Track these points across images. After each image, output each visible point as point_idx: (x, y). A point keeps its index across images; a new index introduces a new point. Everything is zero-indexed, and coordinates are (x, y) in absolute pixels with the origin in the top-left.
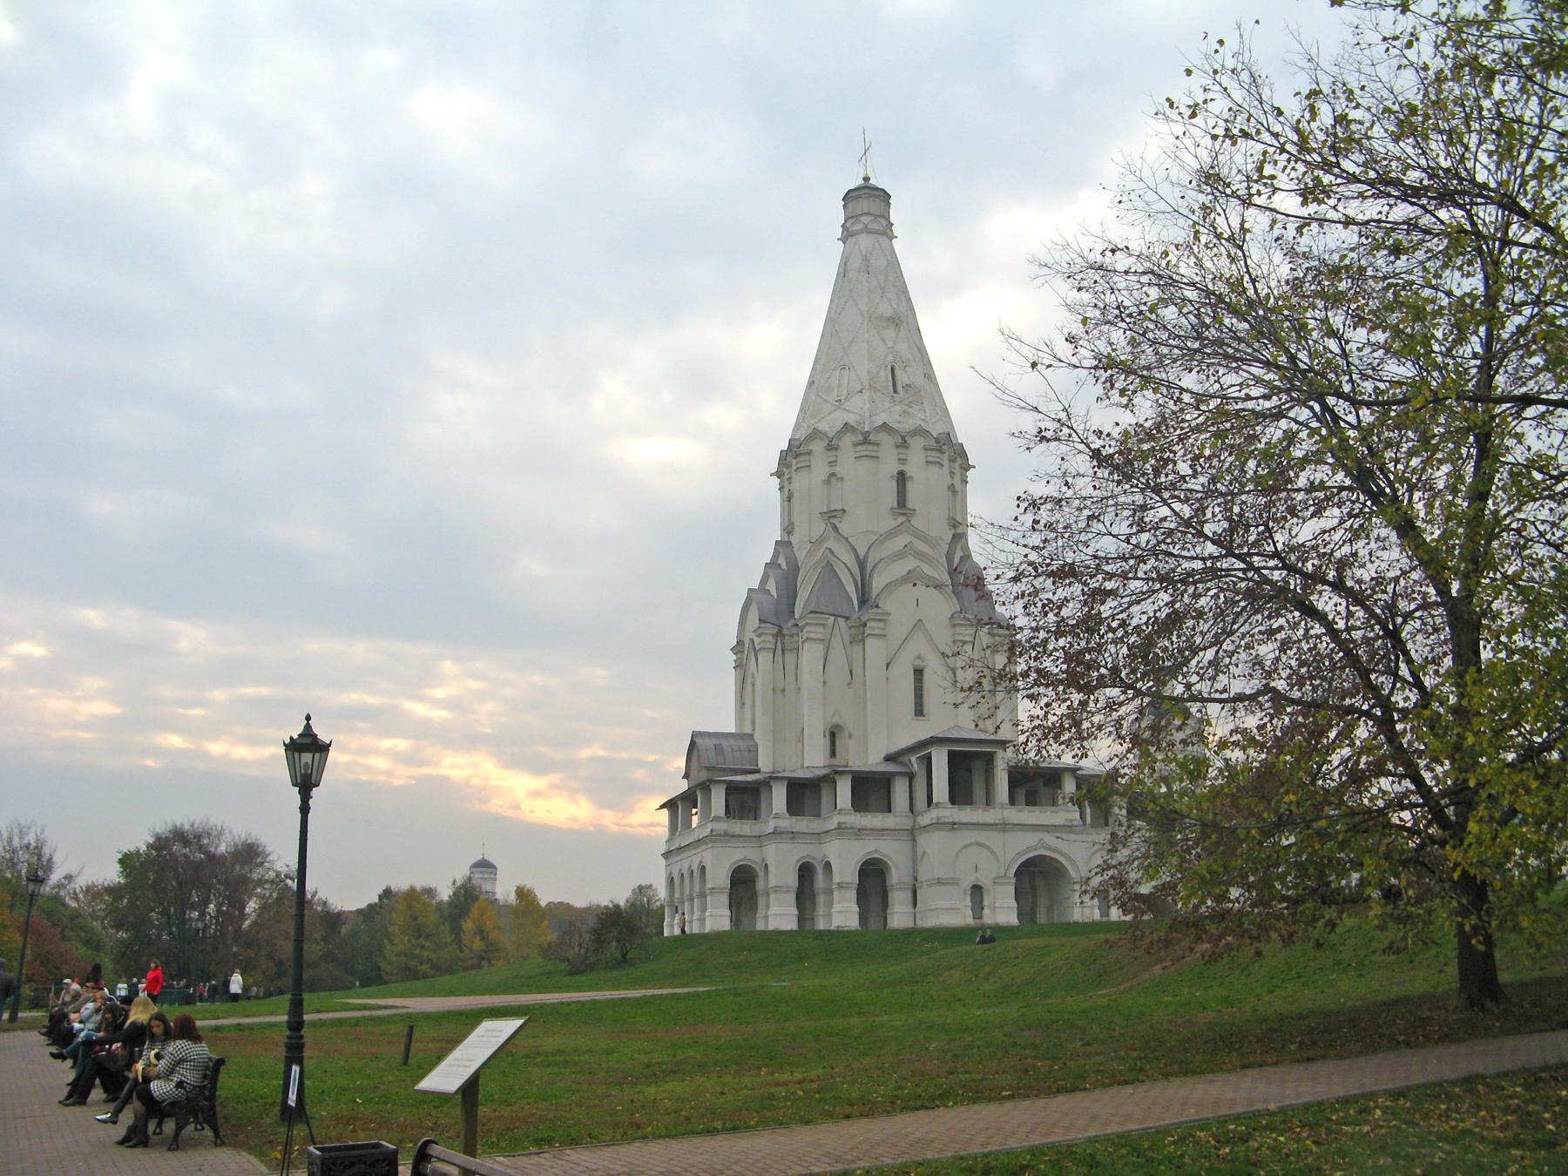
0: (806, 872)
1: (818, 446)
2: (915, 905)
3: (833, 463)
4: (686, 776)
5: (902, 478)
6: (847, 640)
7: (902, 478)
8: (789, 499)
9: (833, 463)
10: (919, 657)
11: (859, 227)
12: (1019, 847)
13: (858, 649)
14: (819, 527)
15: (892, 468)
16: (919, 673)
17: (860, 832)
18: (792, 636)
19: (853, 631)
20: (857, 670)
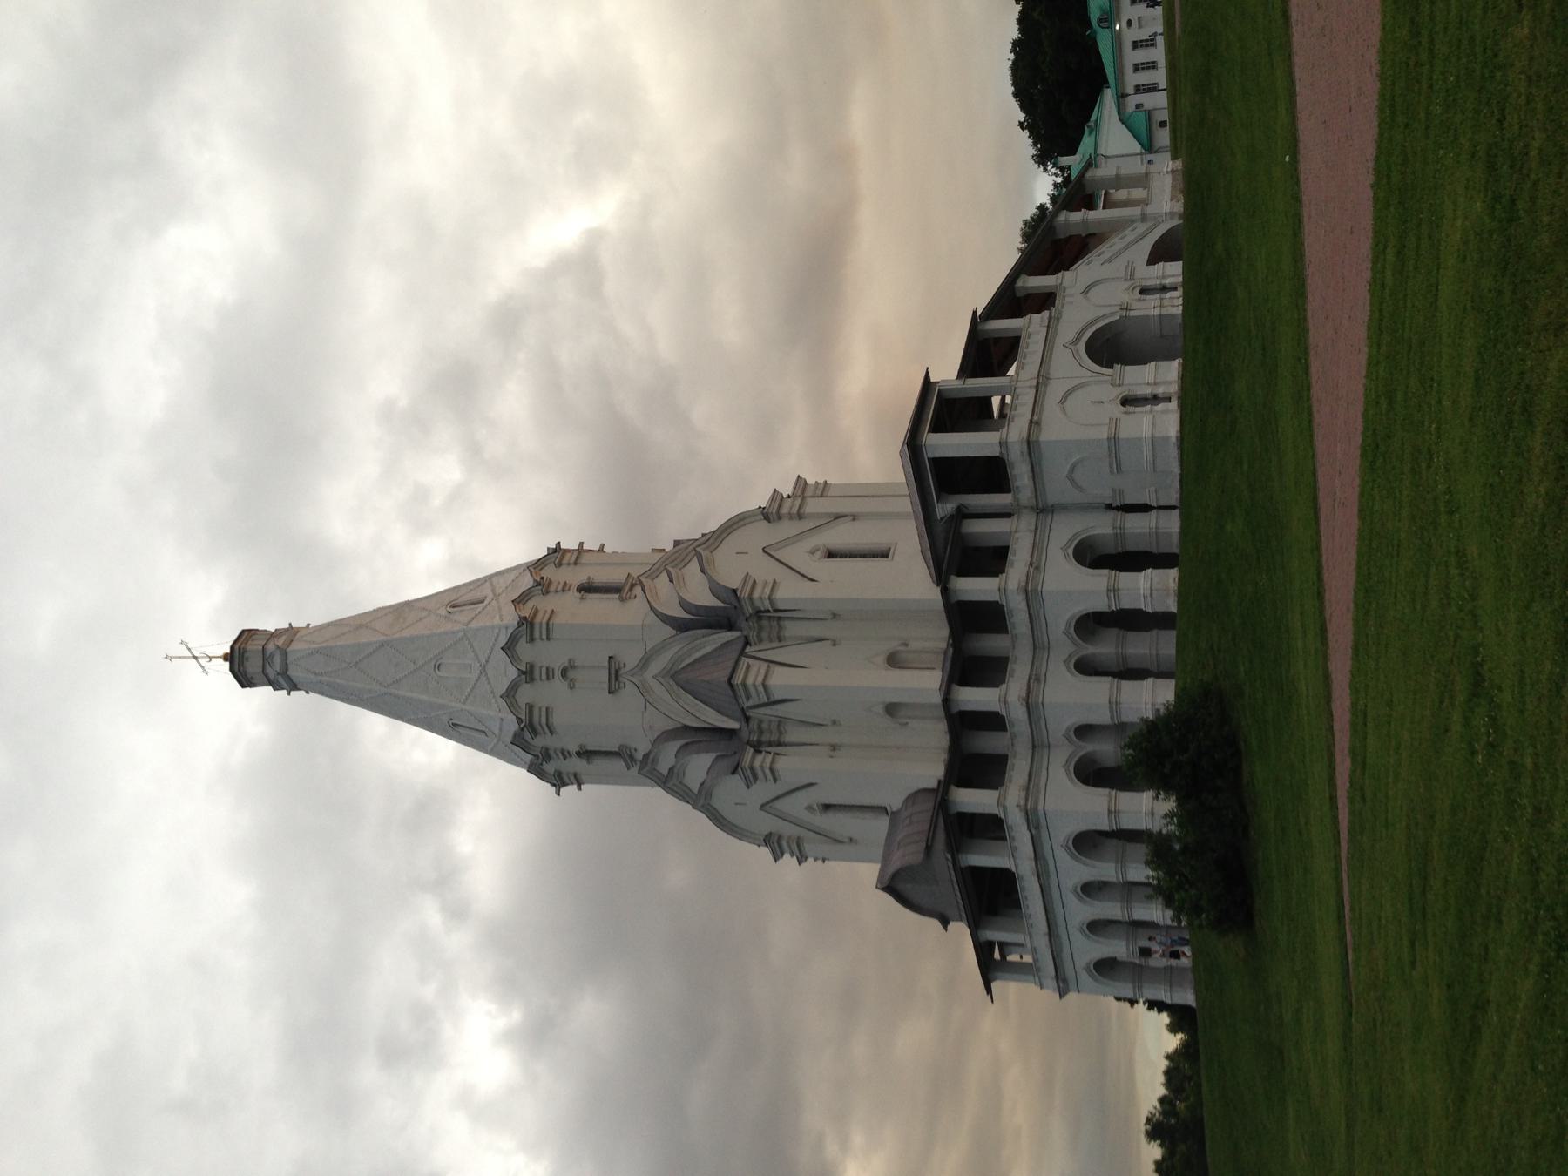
0: (1086, 667)
1: (526, 694)
2: (1144, 508)
3: (549, 674)
4: (945, 922)
5: (587, 589)
6: (775, 644)
7: (587, 589)
8: (586, 754)
9: (549, 674)
10: (812, 552)
11: (277, 660)
12: (1071, 365)
13: (792, 629)
14: (629, 695)
15: (573, 594)
16: (831, 555)
17: (1036, 567)
18: (761, 731)
19: (764, 635)
20: (815, 630)
